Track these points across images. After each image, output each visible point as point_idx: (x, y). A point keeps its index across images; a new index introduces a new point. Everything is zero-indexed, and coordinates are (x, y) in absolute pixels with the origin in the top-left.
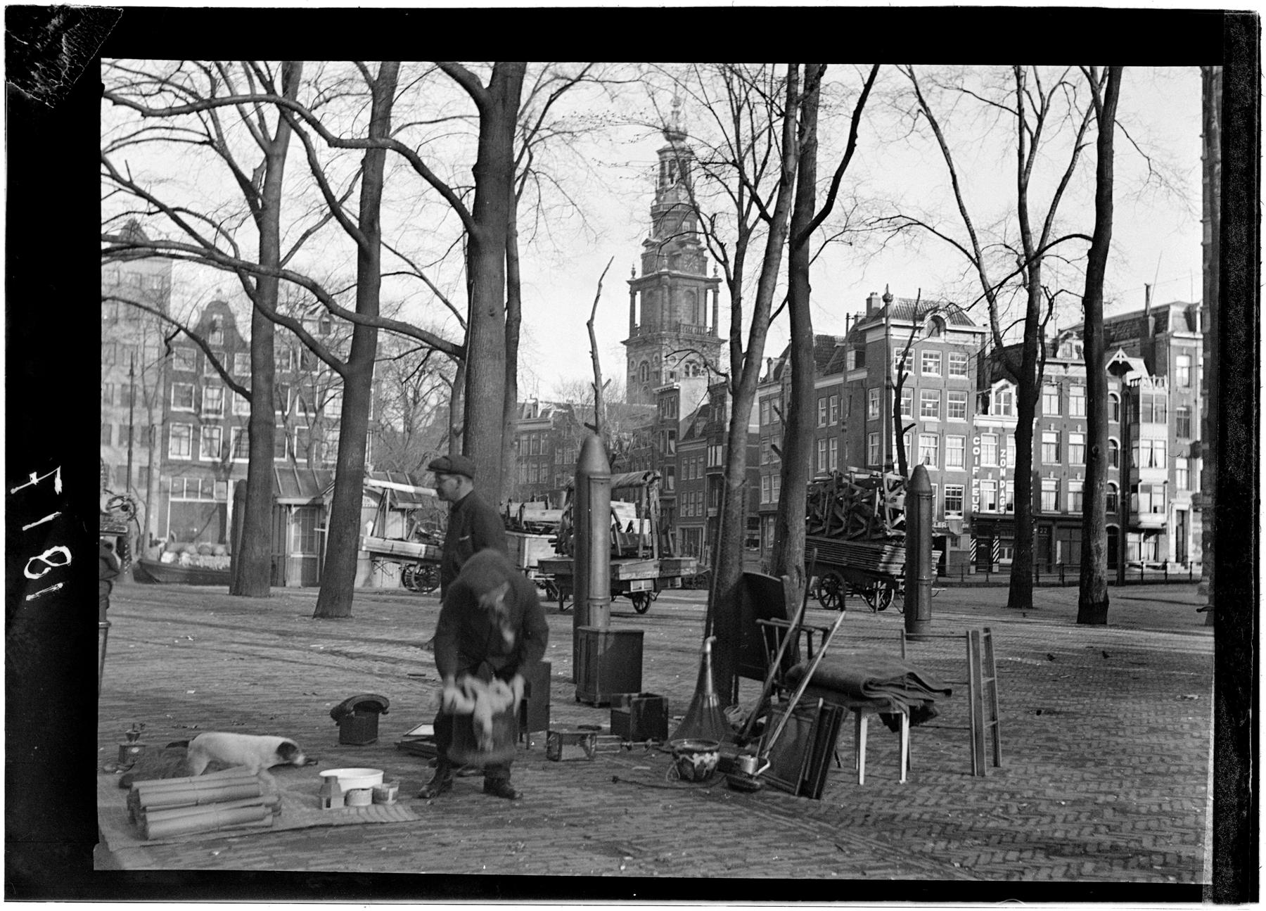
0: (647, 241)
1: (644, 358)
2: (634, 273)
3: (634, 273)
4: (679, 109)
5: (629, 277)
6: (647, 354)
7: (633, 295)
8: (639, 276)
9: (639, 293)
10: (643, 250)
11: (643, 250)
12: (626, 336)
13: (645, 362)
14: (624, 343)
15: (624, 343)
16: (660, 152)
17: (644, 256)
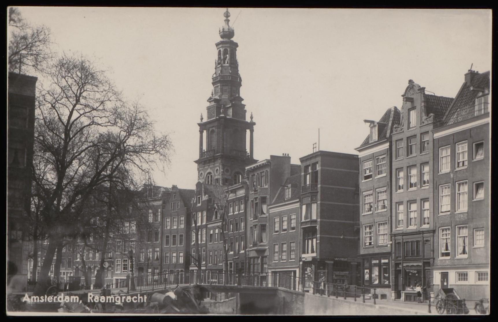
0: (210, 98)
1: (209, 170)
2: (202, 119)
3: (202, 119)
4: (229, 18)
5: (199, 121)
6: (211, 168)
7: (201, 132)
8: (205, 120)
9: (205, 132)
10: (208, 104)
11: (208, 104)
12: (197, 157)
13: (210, 173)
14: (196, 162)
15: (196, 162)
16: (217, 45)
17: (209, 108)
